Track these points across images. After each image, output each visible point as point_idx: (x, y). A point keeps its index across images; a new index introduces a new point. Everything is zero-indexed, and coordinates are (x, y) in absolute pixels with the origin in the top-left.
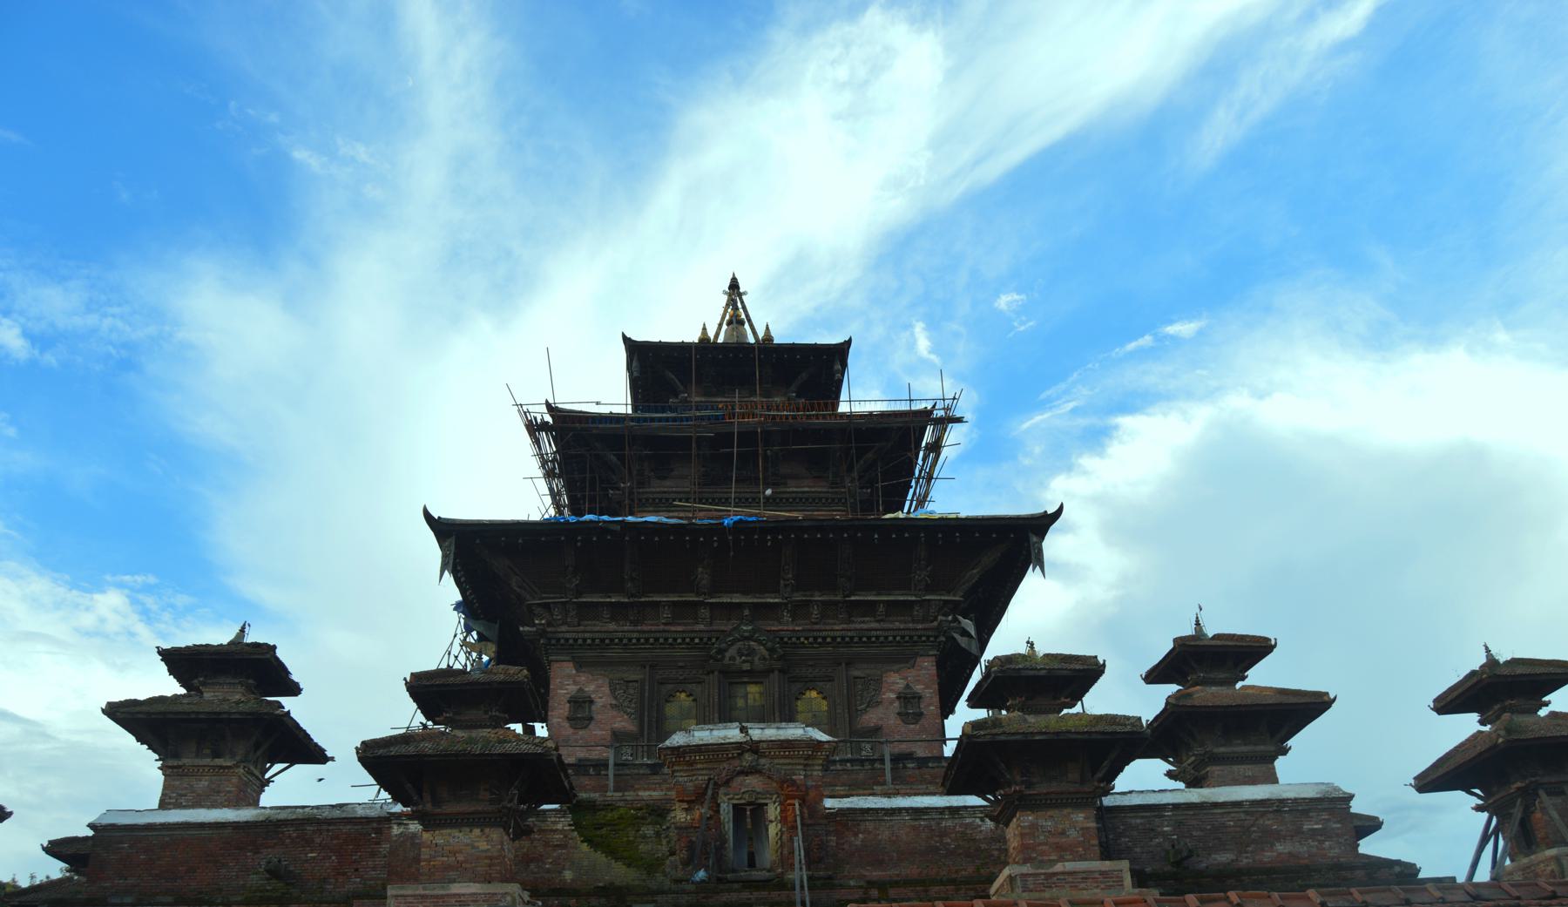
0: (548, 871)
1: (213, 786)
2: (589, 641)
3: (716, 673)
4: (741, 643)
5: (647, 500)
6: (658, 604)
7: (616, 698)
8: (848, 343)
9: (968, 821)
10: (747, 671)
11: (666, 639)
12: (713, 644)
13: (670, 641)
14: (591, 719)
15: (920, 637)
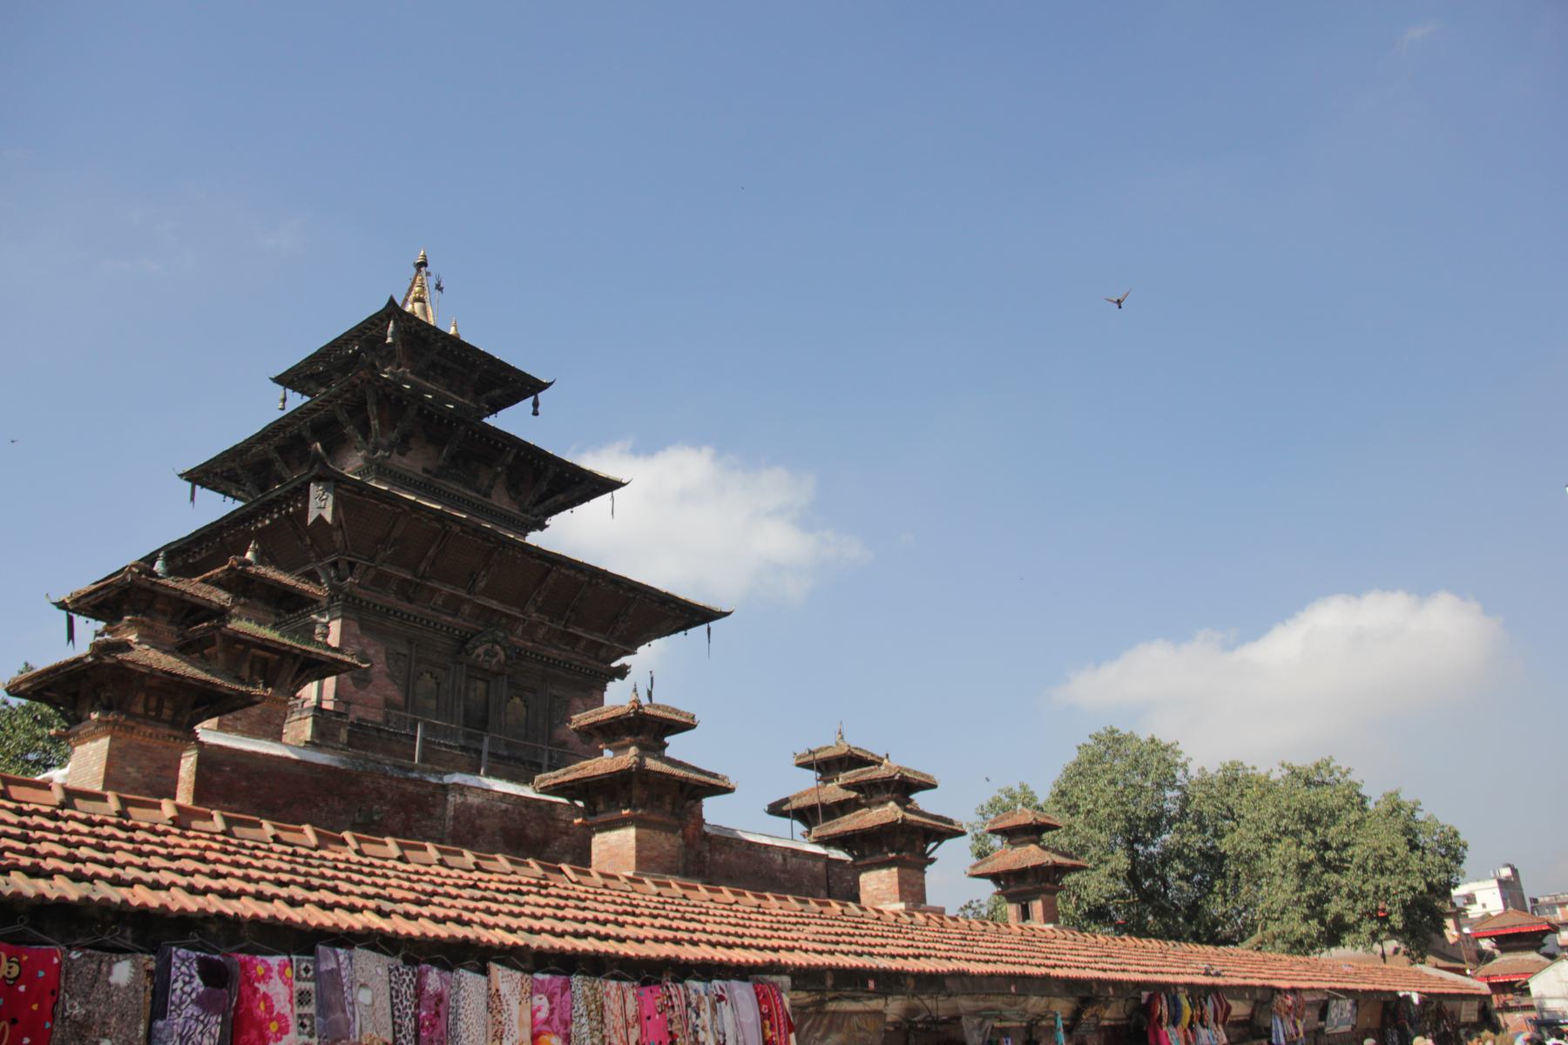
0: (556, 852)
1: (265, 716)
2: (378, 608)
3: (464, 665)
4: (490, 645)
5: (390, 471)
6: (434, 591)
7: (388, 666)
8: (551, 384)
9: (771, 855)
10: (486, 670)
11: (435, 624)
12: (468, 640)
13: (438, 627)
14: (370, 682)
15: (601, 674)
